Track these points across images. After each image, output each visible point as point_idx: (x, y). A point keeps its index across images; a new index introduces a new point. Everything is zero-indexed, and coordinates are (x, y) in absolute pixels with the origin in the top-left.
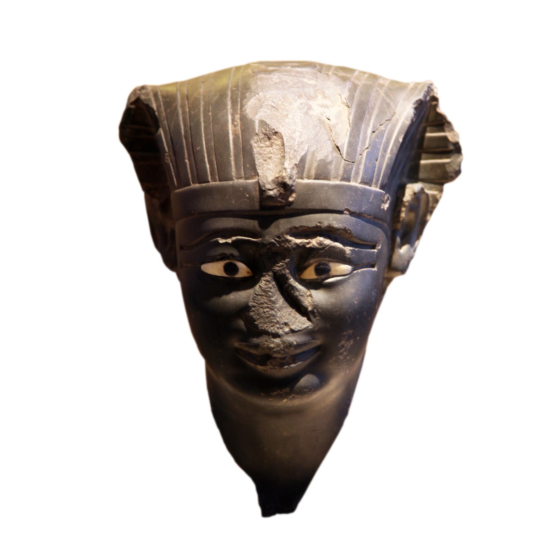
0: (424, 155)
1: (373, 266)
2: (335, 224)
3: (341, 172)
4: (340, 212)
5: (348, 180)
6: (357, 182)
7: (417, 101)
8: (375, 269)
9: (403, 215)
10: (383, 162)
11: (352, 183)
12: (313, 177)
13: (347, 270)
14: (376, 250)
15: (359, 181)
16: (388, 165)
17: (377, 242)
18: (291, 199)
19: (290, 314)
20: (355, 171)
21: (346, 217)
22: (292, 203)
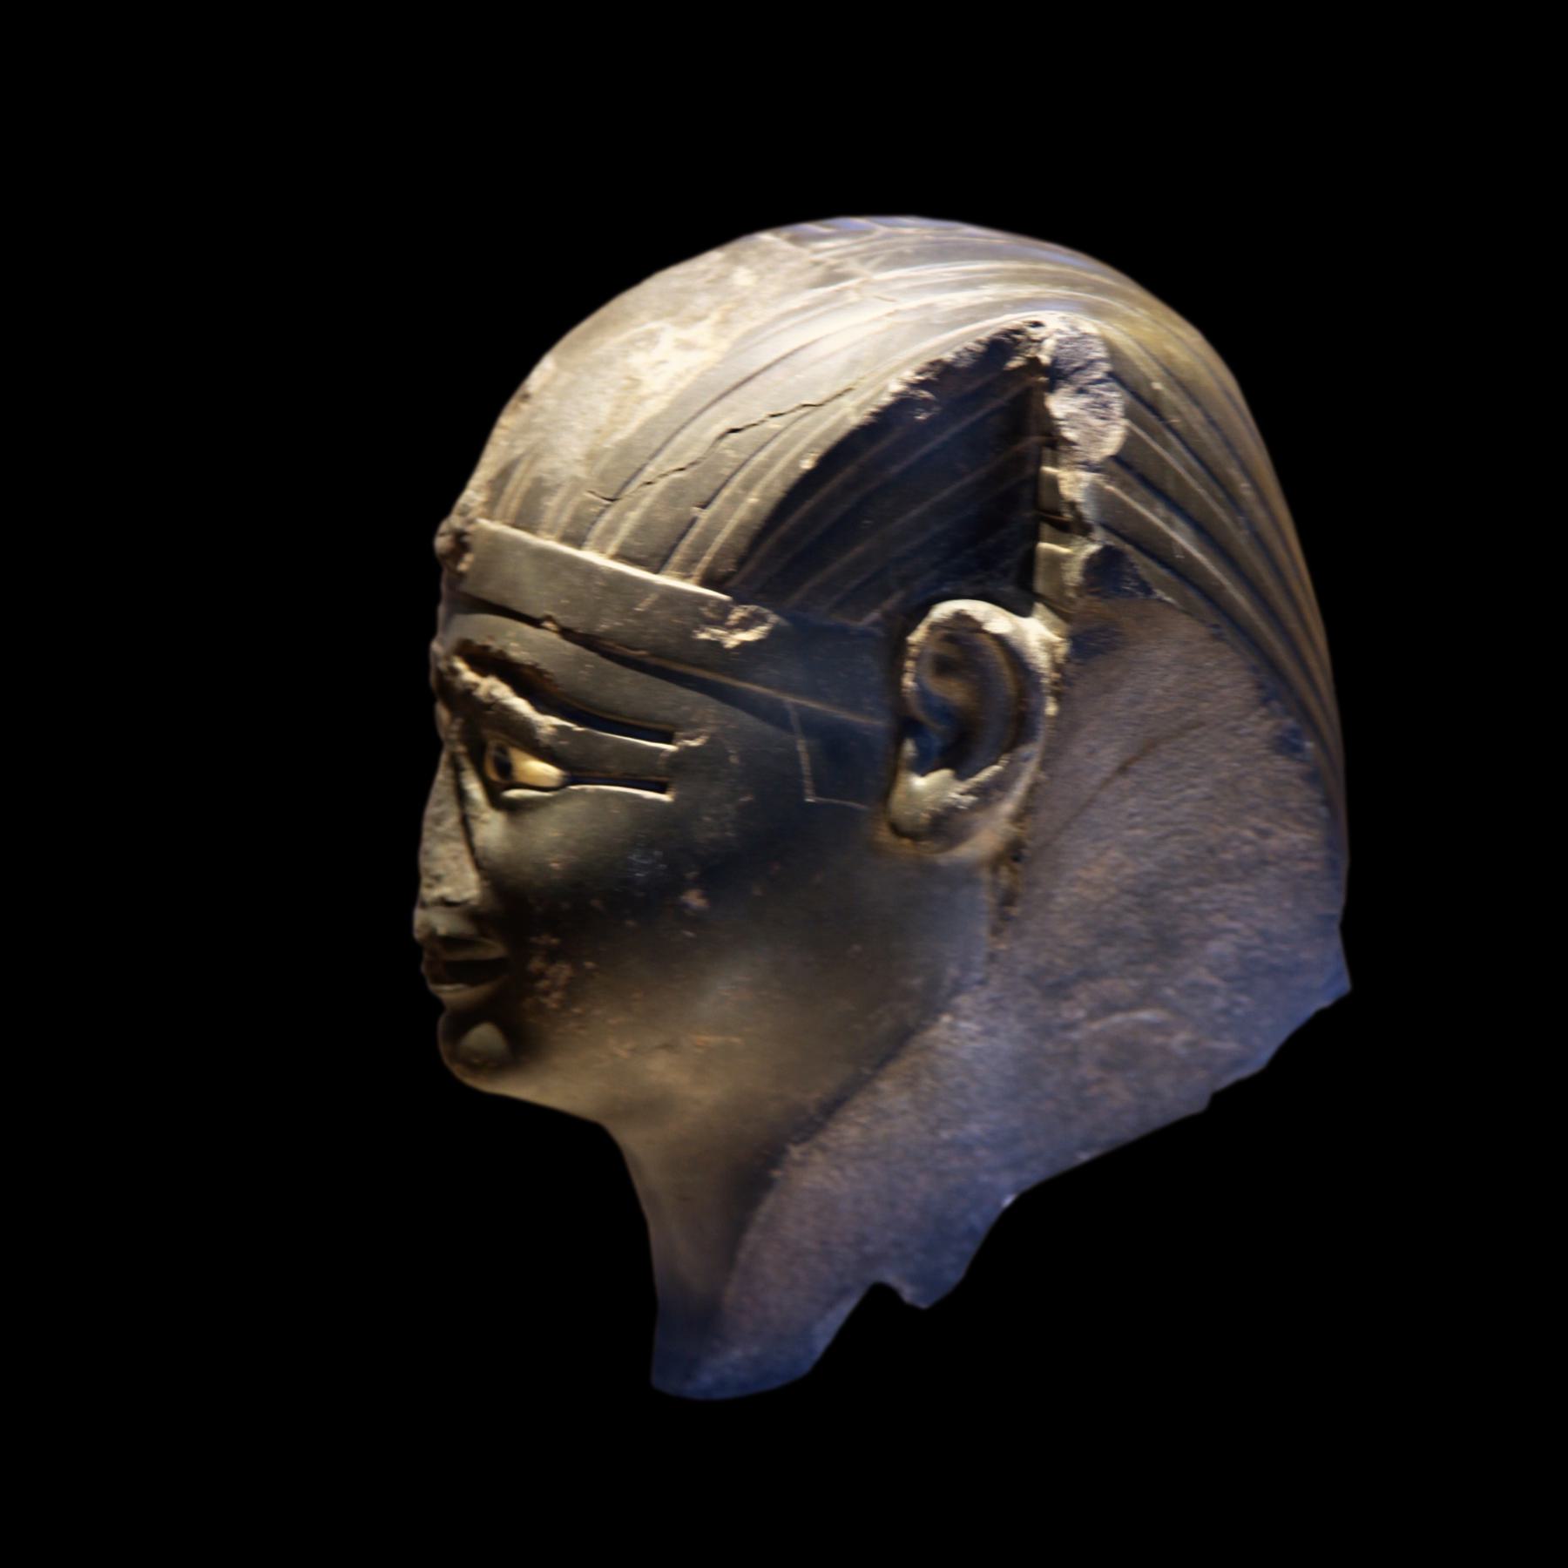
0: (1046, 529)
1: (662, 789)
2: (515, 649)
3: (565, 518)
4: (535, 622)
5: (578, 541)
6: (602, 552)
7: (933, 364)
8: (665, 798)
9: (908, 682)
10: (729, 517)
11: (588, 555)
12: (508, 521)
13: (548, 778)
14: (670, 748)
15: (612, 549)
16: (741, 527)
17: (678, 727)
18: (463, 567)
19: (455, 858)
20: (610, 522)
21: (547, 636)
22: (462, 575)
